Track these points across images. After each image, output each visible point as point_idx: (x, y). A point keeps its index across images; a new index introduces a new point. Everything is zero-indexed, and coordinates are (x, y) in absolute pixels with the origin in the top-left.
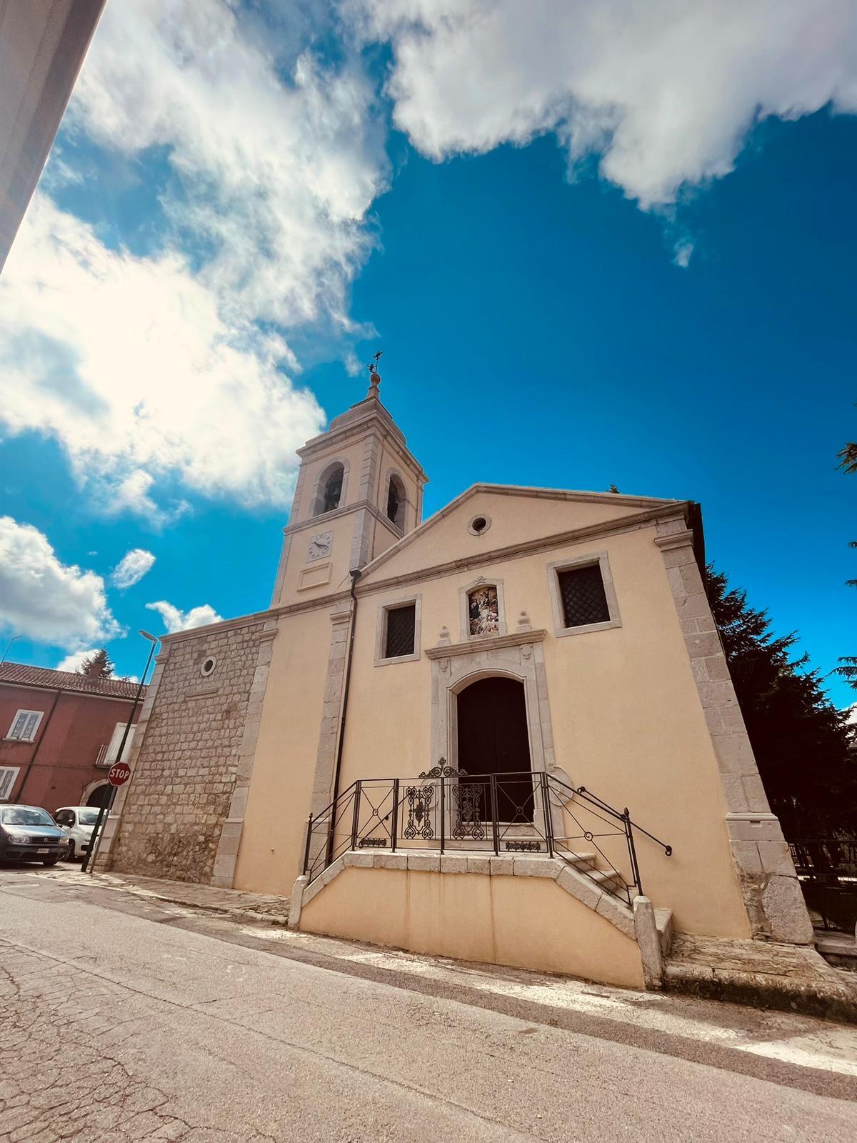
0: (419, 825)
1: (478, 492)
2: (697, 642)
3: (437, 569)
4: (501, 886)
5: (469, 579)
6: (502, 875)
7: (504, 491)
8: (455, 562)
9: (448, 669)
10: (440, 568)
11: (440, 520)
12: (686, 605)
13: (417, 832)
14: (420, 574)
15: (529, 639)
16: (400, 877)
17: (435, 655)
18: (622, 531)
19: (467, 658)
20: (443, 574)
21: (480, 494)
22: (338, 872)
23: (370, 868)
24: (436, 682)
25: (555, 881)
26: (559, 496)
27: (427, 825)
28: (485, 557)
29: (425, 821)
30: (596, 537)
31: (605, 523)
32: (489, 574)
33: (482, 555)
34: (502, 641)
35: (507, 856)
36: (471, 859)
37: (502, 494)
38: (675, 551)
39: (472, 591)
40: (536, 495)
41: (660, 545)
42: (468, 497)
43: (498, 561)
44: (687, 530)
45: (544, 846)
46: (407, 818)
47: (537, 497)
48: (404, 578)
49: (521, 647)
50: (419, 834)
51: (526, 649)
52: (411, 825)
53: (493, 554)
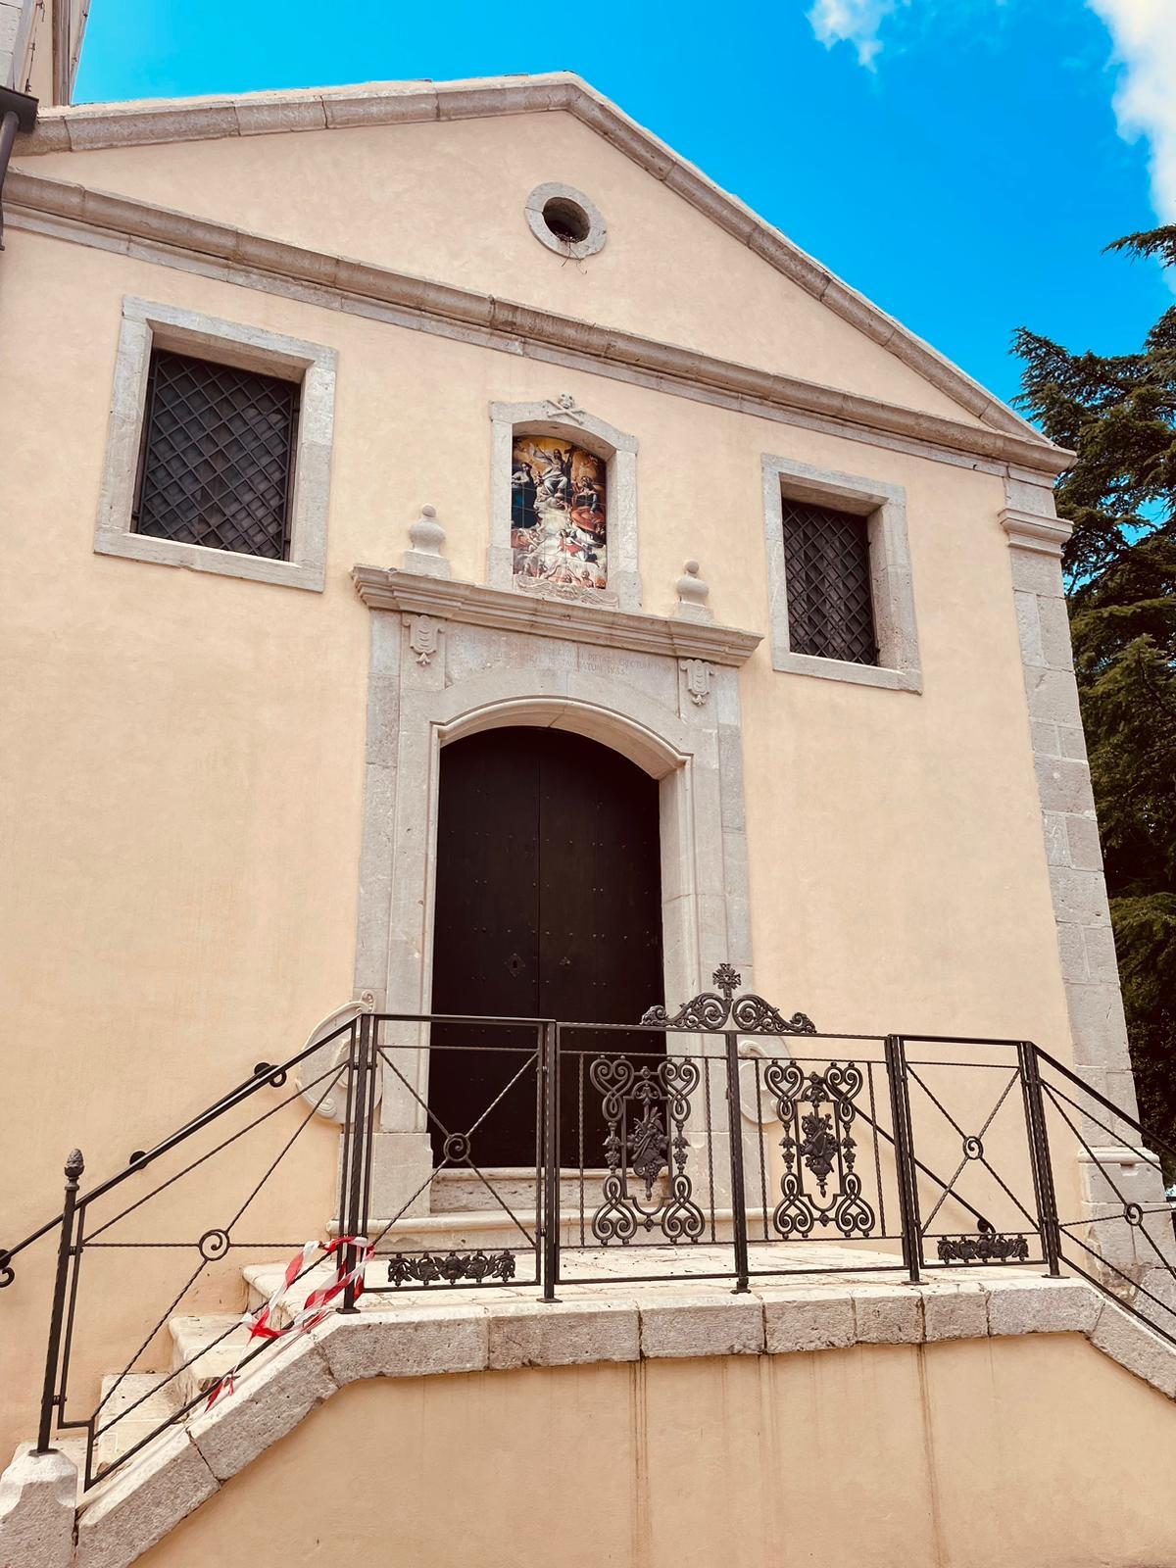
0: (824, 1192)
1: (568, 108)
2: (1056, 775)
3: (418, 292)
4: (957, 1374)
5: (537, 388)
6: (958, 1338)
7: (662, 164)
8: (493, 302)
9: (440, 659)
10: (432, 295)
11: (420, 118)
12: (1042, 687)
13: (817, 1214)
14: (343, 274)
15: (694, 649)
16: (610, 1389)
17: (389, 597)
18: (941, 456)
19: (507, 643)
20: (430, 324)
21: (571, 120)
22: (299, 1411)
23: (471, 1375)
24: (387, 698)
25: (1088, 1339)
26: (810, 277)
27: (851, 1188)
28: (597, 340)
29: (842, 1178)
30: (884, 442)
31: (918, 416)
32: (605, 406)
33: (591, 328)
34: (637, 630)
35: (946, 1282)
36: (867, 1300)
37: (648, 168)
38: (1034, 555)
39: (531, 431)
40: (750, 237)
41: (1008, 530)
42: (536, 104)
43: (625, 373)
44: (1056, 518)
45: (526, 1266)
46: (777, 1168)
47: (748, 242)
48: (270, 254)
49: (683, 664)
50: (825, 1221)
51: (697, 675)
52: (793, 1189)
53: (621, 345)
